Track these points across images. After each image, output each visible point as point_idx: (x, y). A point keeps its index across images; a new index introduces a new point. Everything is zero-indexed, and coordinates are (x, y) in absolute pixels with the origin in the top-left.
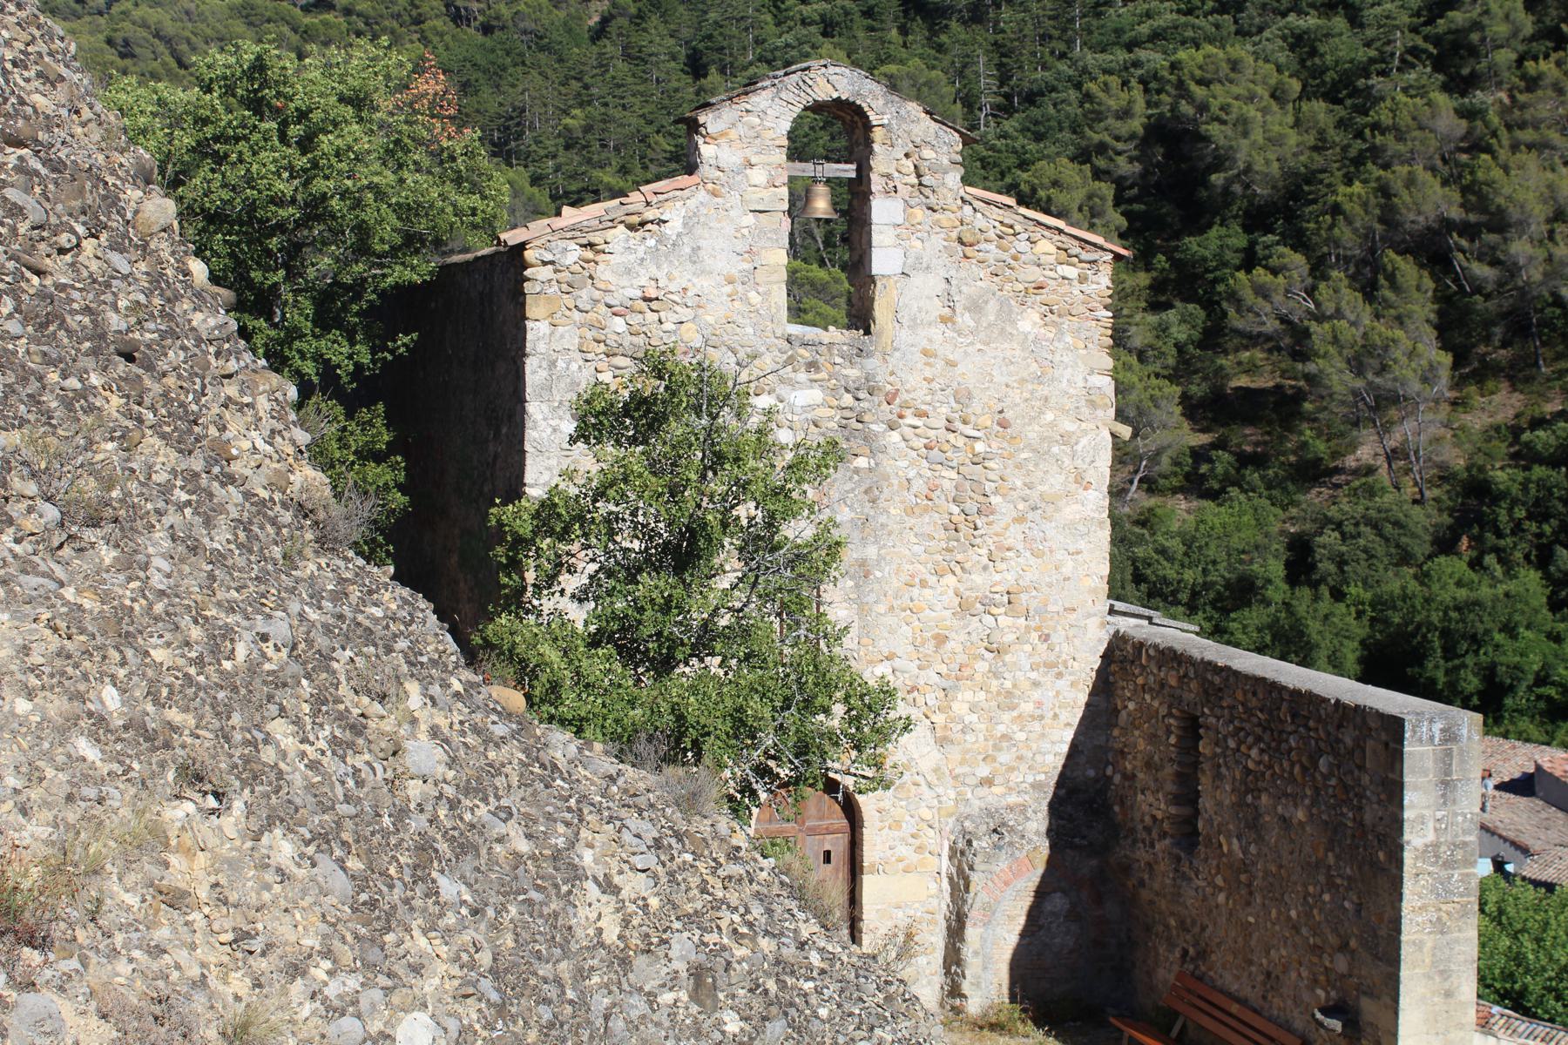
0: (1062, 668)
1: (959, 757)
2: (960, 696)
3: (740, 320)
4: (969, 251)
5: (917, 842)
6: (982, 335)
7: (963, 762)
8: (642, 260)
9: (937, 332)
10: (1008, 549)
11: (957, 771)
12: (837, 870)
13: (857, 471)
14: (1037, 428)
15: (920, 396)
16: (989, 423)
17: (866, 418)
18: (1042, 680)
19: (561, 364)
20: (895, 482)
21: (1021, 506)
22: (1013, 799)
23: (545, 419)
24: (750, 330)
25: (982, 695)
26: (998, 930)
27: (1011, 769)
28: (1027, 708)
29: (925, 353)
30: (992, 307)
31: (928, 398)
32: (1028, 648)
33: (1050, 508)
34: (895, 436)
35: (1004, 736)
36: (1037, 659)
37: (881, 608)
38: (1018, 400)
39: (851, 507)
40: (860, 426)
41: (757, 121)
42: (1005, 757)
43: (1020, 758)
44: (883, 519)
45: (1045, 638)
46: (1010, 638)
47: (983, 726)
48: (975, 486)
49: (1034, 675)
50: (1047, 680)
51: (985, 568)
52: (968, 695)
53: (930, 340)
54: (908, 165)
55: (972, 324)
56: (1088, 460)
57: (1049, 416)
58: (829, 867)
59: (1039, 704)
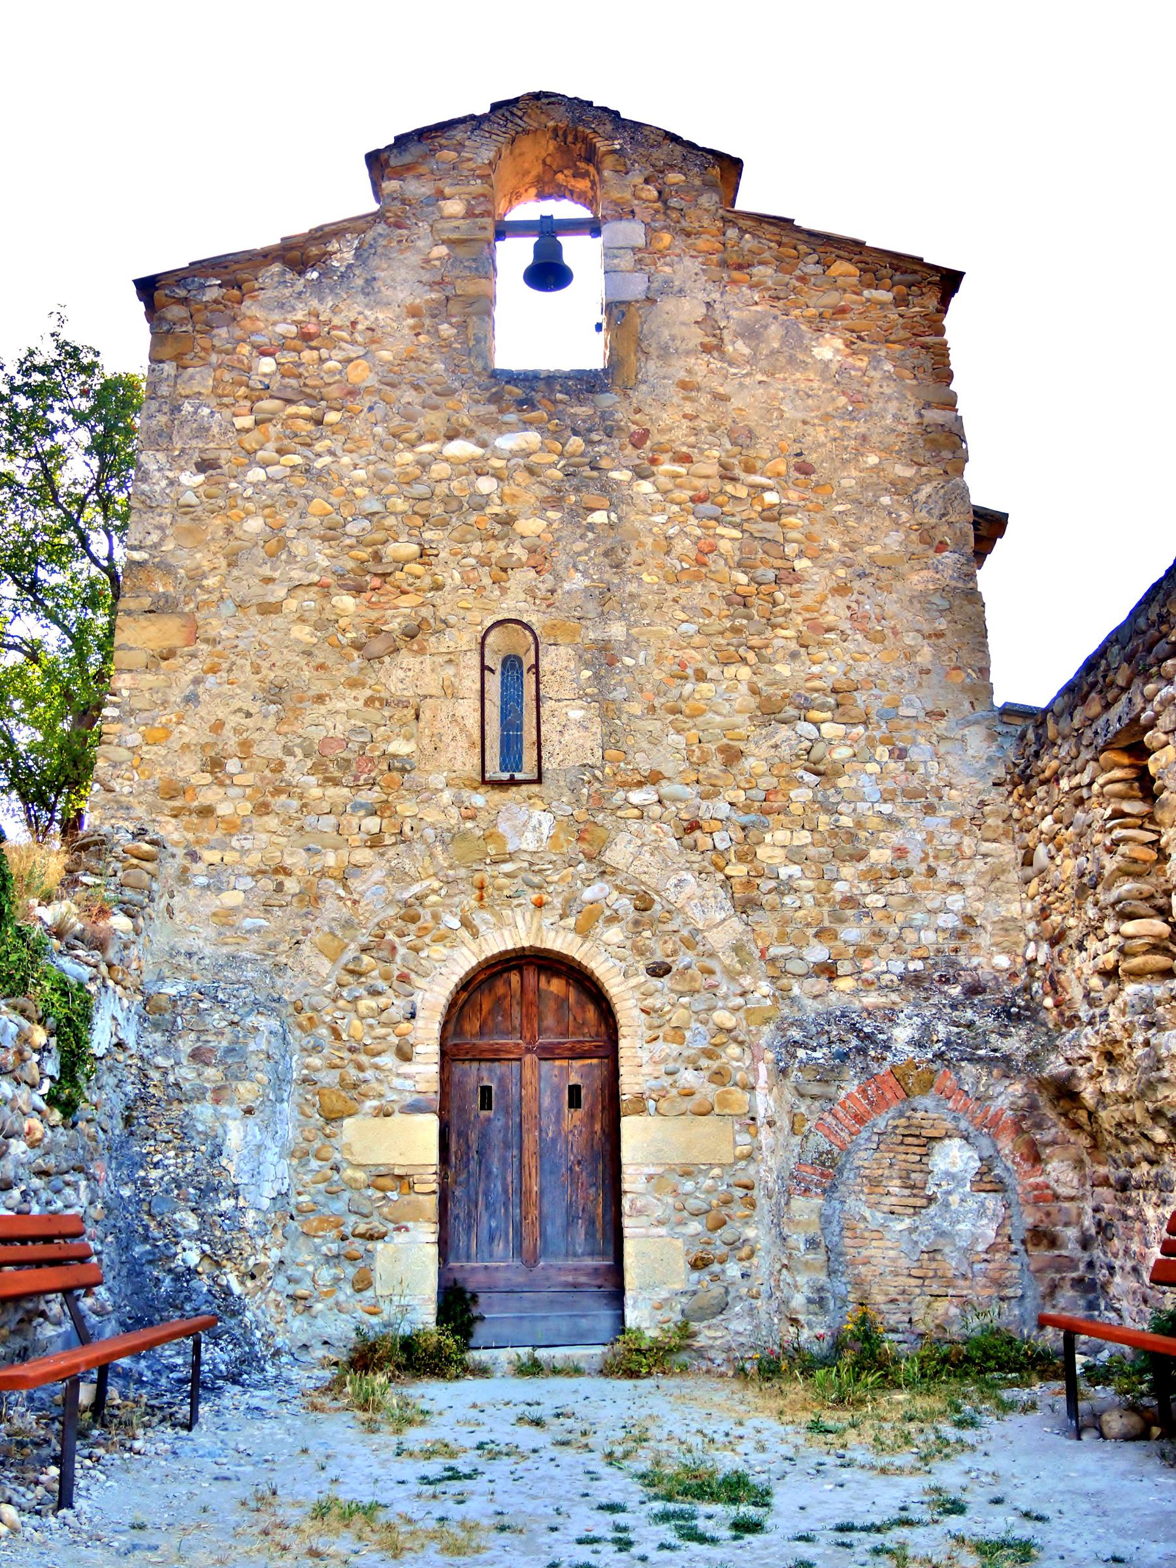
0: (933, 799)
1: (775, 931)
2: (768, 838)
3: (426, 353)
4: (736, 275)
5: (715, 1065)
6: (763, 364)
7: (782, 937)
8: (300, 293)
9: (700, 365)
10: (829, 630)
11: (773, 951)
12: (591, 1116)
13: (591, 527)
14: (854, 473)
15: (680, 437)
16: (782, 468)
17: (604, 463)
18: (901, 815)
19: (187, 408)
20: (649, 541)
21: (841, 573)
22: (872, 999)
23: (160, 470)
24: (439, 366)
25: (804, 837)
26: (851, 1202)
27: (867, 952)
28: (880, 856)
29: (684, 385)
30: (774, 330)
31: (692, 439)
32: (872, 768)
33: (885, 575)
34: (646, 487)
35: (850, 901)
36: (889, 784)
37: (636, 708)
38: (822, 439)
39: (585, 574)
40: (595, 474)
41: (453, 154)
42: (851, 933)
43: (878, 934)
44: (632, 587)
45: (901, 755)
46: (842, 753)
47: (810, 884)
48: (768, 546)
49: (887, 808)
50: (911, 814)
51: (794, 656)
52: (781, 836)
53: (689, 371)
54: (651, 192)
55: (746, 351)
56: (936, 512)
57: (872, 460)
58: (579, 1113)
59: (901, 852)
